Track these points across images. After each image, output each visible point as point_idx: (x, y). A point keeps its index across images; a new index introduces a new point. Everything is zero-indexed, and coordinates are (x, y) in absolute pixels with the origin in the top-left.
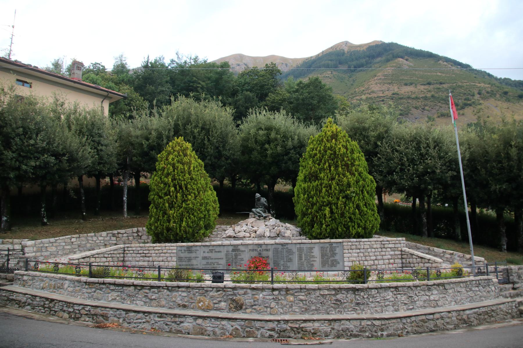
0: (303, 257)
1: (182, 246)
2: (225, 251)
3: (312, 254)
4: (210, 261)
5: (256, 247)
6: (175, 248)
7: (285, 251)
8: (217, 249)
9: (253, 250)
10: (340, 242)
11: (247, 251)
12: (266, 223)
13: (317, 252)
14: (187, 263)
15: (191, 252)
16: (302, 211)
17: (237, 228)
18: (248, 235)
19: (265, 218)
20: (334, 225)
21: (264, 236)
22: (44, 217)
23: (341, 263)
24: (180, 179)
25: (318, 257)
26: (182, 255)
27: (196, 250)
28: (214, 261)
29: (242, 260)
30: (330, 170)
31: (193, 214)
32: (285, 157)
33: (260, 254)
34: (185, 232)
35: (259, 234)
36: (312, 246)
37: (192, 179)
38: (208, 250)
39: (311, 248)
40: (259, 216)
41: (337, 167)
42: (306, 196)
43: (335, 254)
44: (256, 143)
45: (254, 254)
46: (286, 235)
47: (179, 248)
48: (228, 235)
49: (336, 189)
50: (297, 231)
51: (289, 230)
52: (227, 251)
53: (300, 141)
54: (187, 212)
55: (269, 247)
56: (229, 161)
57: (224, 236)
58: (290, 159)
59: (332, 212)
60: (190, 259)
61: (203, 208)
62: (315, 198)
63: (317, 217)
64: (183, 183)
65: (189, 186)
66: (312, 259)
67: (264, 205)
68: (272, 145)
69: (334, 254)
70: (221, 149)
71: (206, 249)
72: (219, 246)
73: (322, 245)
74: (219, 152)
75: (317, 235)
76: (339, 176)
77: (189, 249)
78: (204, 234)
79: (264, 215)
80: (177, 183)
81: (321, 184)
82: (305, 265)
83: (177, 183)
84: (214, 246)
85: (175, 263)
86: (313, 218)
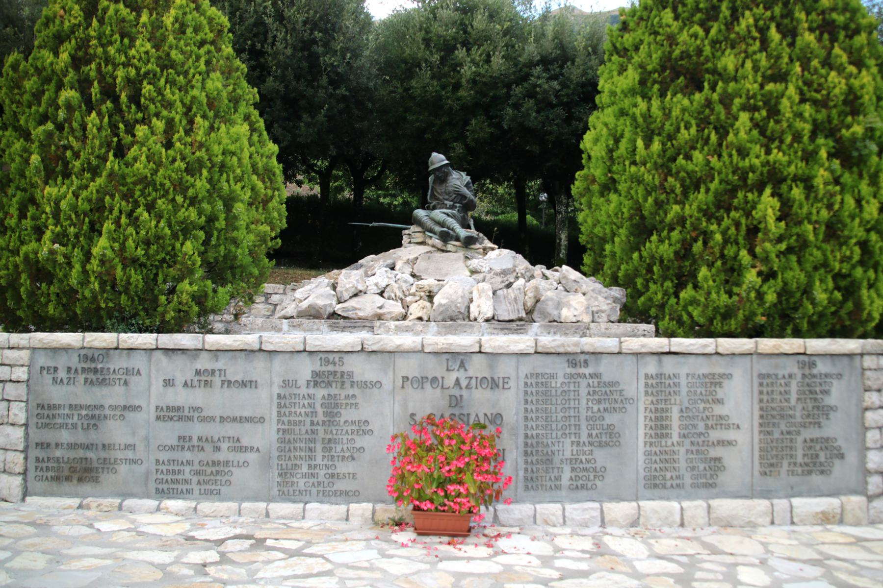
1: (55, 350)
2: (277, 381)
3: (718, 410)
4: (197, 430)
5: (434, 368)
6: (25, 355)
7: (583, 391)
8: (236, 370)
9: (421, 382)
10: (850, 356)
12: (475, 263)
13: (739, 400)
14: (80, 437)
15: (103, 382)
16: (638, 208)
17: (348, 278)
18: (396, 308)
19: (469, 242)
20: (795, 275)
21: (467, 316)
23: (852, 457)
24: (108, 60)
25: (745, 426)
26: (57, 394)
27: (128, 371)
28: (215, 430)
29: (363, 428)
30: (765, 44)
31: (150, 207)
32: (517, 90)
33: (456, 402)
34: (108, 281)
35: (446, 308)
36: (718, 367)
37: (166, 64)
38: (190, 375)
39: (715, 381)
40: (446, 237)
41: (790, 33)
42: (656, 146)
43: (826, 411)
44: (428, 46)
45: (427, 402)
46: (566, 314)
47: (42, 360)
48: (305, 305)
49: (800, 115)
50: (616, 300)
51: (579, 298)
52: (286, 384)
53: (561, 42)
54: (125, 197)
55: (505, 369)
56: (343, 91)
57: (291, 310)
58: (531, 94)
59: (784, 215)
60: (94, 417)
61: (201, 184)
62: (698, 156)
63: (707, 236)
64: (120, 73)
65: (147, 88)
66: (714, 435)
67: (464, 197)
68: (477, 54)
69: (818, 412)
70: (320, 50)
71: (182, 370)
72: (247, 352)
73: (764, 366)
74: (313, 59)
75: (711, 320)
76: (805, 67)
77: (93, 367)
78: (199, 299)
79: (463, 233)
80: (93, 74)
81: (726, 100)
82: (682, 464)
83: (93, 74)
84: (217, 352)
85: (20, 433)
86: (687, 246)
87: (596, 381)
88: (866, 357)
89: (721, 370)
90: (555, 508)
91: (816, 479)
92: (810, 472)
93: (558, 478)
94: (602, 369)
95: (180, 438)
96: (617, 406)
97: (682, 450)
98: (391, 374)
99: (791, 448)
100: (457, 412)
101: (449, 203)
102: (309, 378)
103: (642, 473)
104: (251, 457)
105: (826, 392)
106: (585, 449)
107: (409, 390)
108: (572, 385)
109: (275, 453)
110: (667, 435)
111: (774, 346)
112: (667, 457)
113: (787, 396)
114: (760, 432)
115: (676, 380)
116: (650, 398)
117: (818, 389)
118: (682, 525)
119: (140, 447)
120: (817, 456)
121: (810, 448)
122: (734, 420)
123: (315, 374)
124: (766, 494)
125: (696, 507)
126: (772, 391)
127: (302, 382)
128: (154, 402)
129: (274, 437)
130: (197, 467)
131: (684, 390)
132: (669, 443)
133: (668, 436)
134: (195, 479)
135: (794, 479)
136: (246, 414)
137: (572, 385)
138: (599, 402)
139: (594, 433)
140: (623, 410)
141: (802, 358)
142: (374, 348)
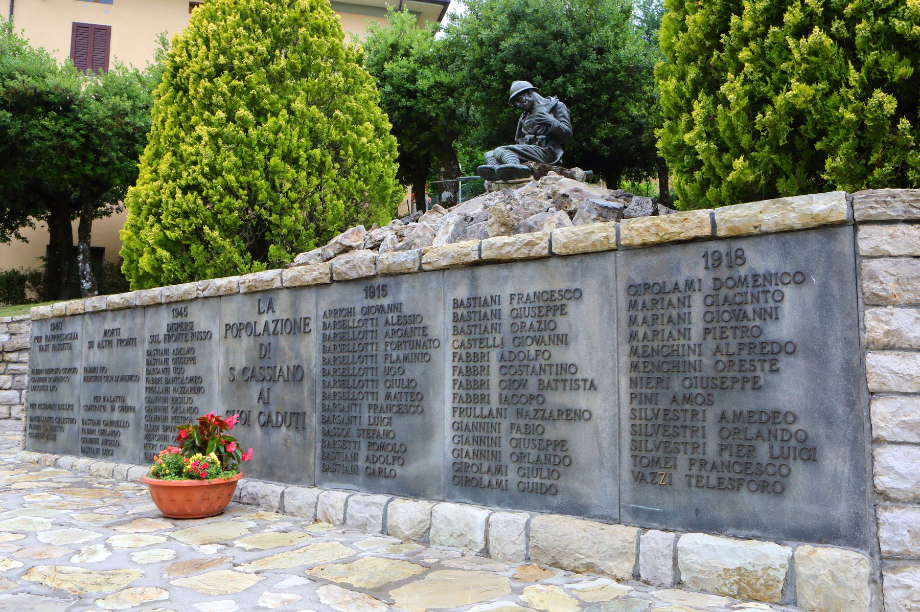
0: (494, 377)
2: (148, 338)
3: (560, 355)
10: (827, 228)
11: (216, 336)
22: (84, 277)
23: (835, 461)
33: (265, 351)
36: (556, 279)
39: (552, 305)
52: (154, 339)
66: (558, 399)
82: (506, 449)
87: (395, 315)
88: (863, 231)
89: (563, 285)
90: (51, 458)
91: (750, 501)
92: (736, 485)
93: (355, 457)
94: (402, 297)
95: (97, 398)
96: (418, 351)
97: (505, 424)
98: (218, 321)
99: (694, 430)
100: (266, 363)
101: (528, 137)
102: (166, 333)
103: (450, 458)
104: (131, 416)
105: (773, 315)
106: (383, 415)
107: (230, 339)
108: (370, 322)
109: (144, 413)
110: (483, 397)
111: (647, 230)
112: (483, 434)
113: (683, 326)
114: (633, 396)
115: (495, 307)
116: (460, 338)
117: (749, 309)
118: (486, 552)
119: (76, 409)
120: (752, 449)
121: (737, 431)
122: (587, 373)
123: (170, 328)
124: (646, 519)
125: (507, 523)
126: (655, 318)
127: (161, 338)
128: (84, 364)
129: (144, 395)
130: (102, 427)
131: (506, 321)
132: (486, 412)
133: (484, 399)
134: (101, 438)
135: (703, 497)
136: (129, 373)
137: (370, 322)
138: (398, 346)
139: (393, 391)
140: (425, 357)
141: (712, 246)
142: (206, 294)
